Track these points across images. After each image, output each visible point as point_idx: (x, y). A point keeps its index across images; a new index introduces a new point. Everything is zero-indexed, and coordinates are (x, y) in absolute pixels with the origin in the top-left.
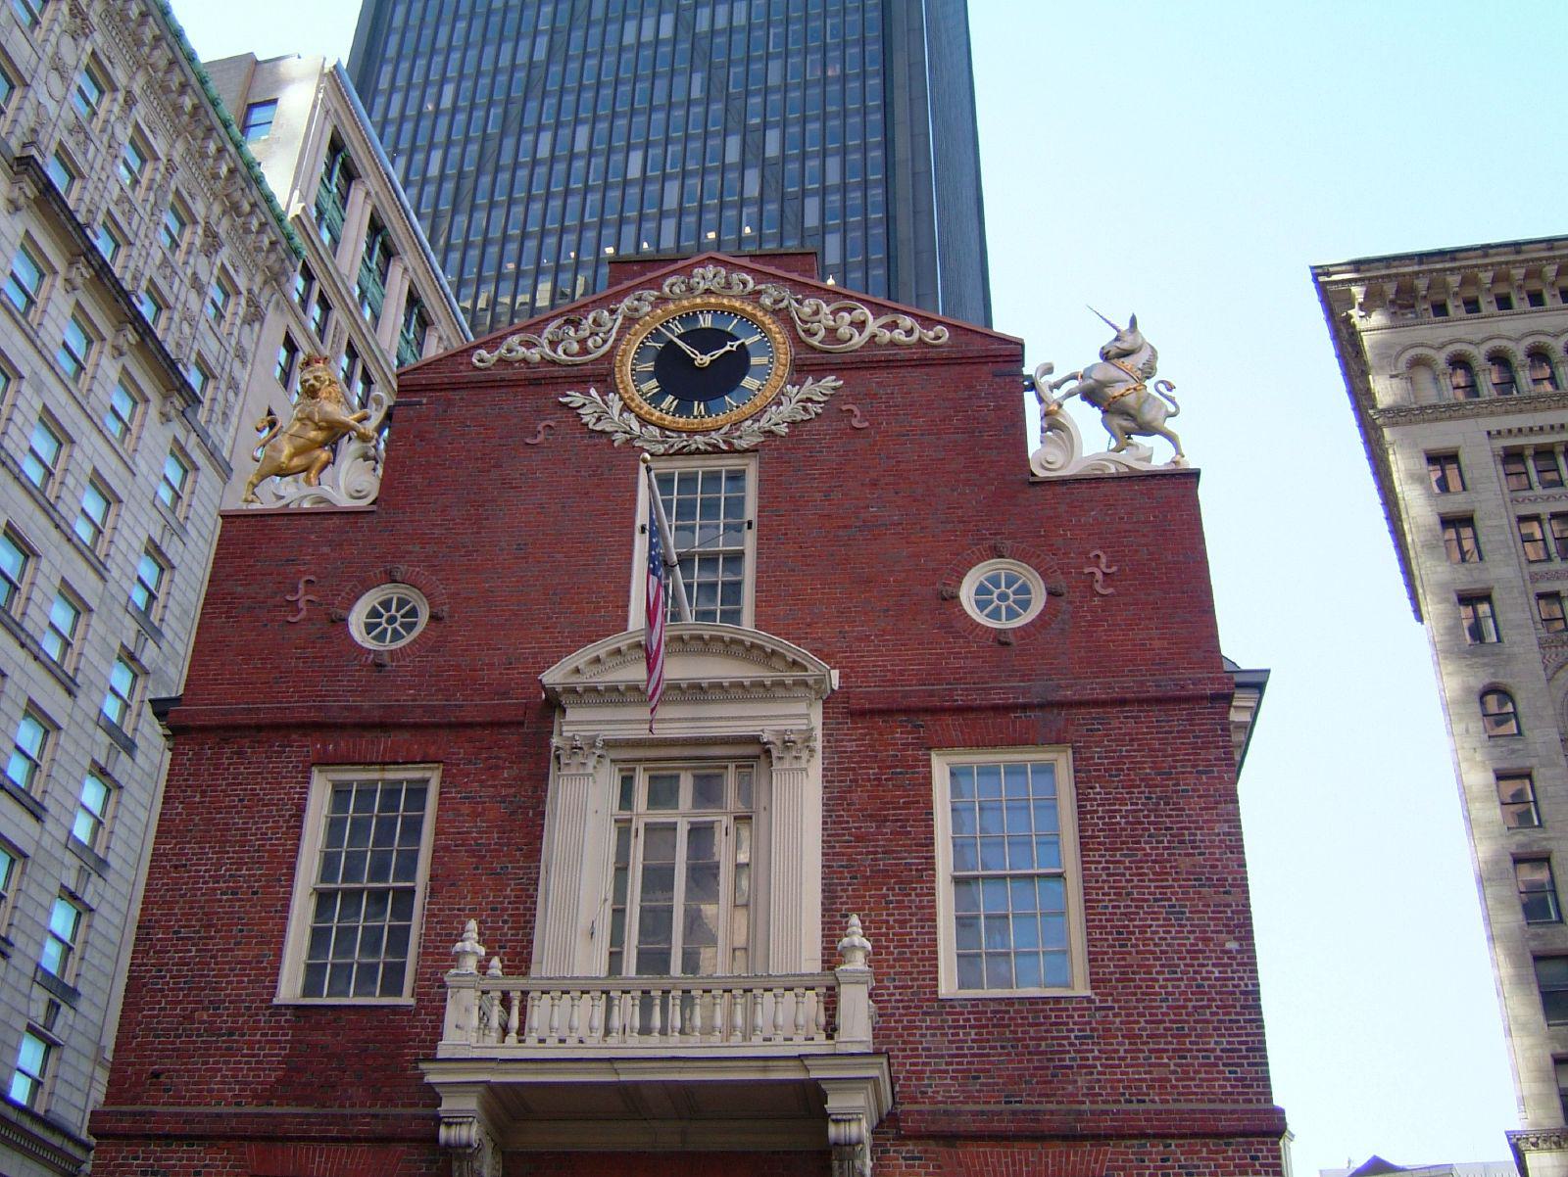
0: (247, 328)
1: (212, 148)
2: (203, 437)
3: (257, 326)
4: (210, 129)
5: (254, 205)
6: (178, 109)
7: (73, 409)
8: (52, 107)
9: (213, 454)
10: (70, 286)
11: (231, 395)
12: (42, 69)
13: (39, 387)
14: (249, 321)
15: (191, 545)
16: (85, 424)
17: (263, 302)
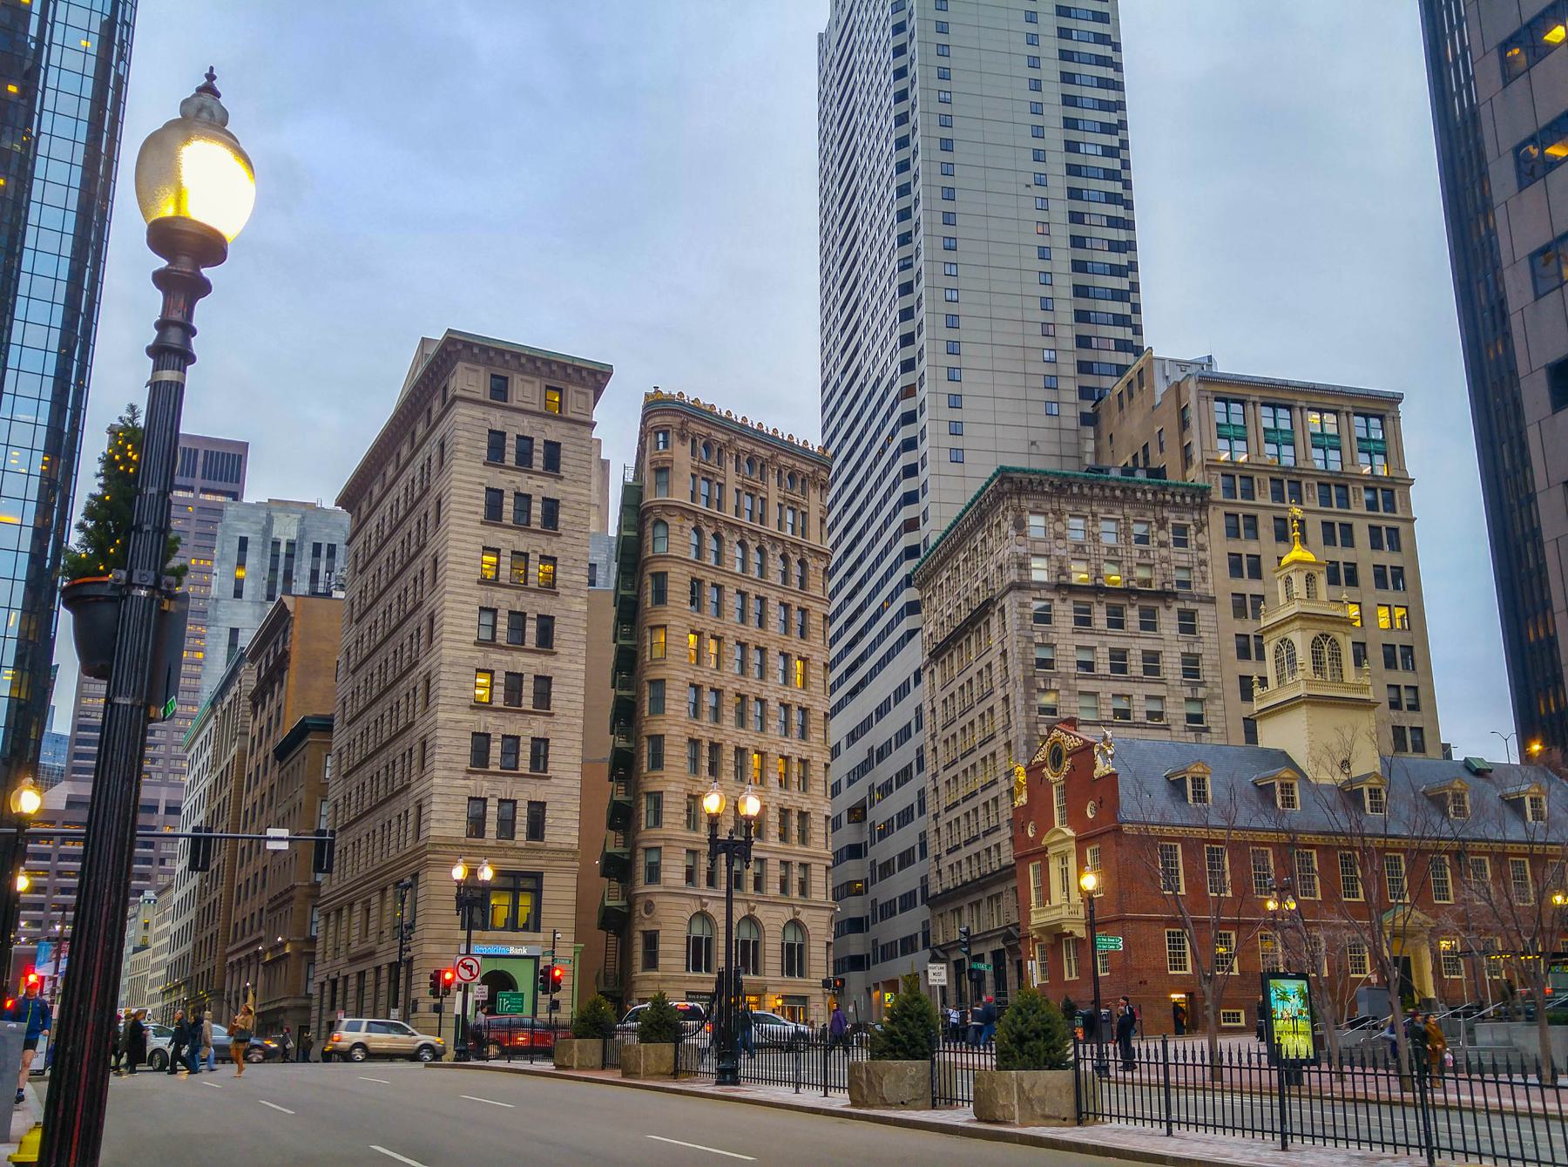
0: (1200, 535)
1: (1139, 495)
2: (1192, 597)
3: (1206, 529)
4: (1134, 492)
5: (1173, 495)
6: (1115, 498)
7: (1122, 640)
8: (1063, 552)
9: (1201, 601)
10: (1100, 603)
11: (1203, 568)
12: (1053, 546)
13: (1103, 644)
14: (1200, 531)
15: (1206, 640)
16: (1130, 640)
17: (1204, 517)
